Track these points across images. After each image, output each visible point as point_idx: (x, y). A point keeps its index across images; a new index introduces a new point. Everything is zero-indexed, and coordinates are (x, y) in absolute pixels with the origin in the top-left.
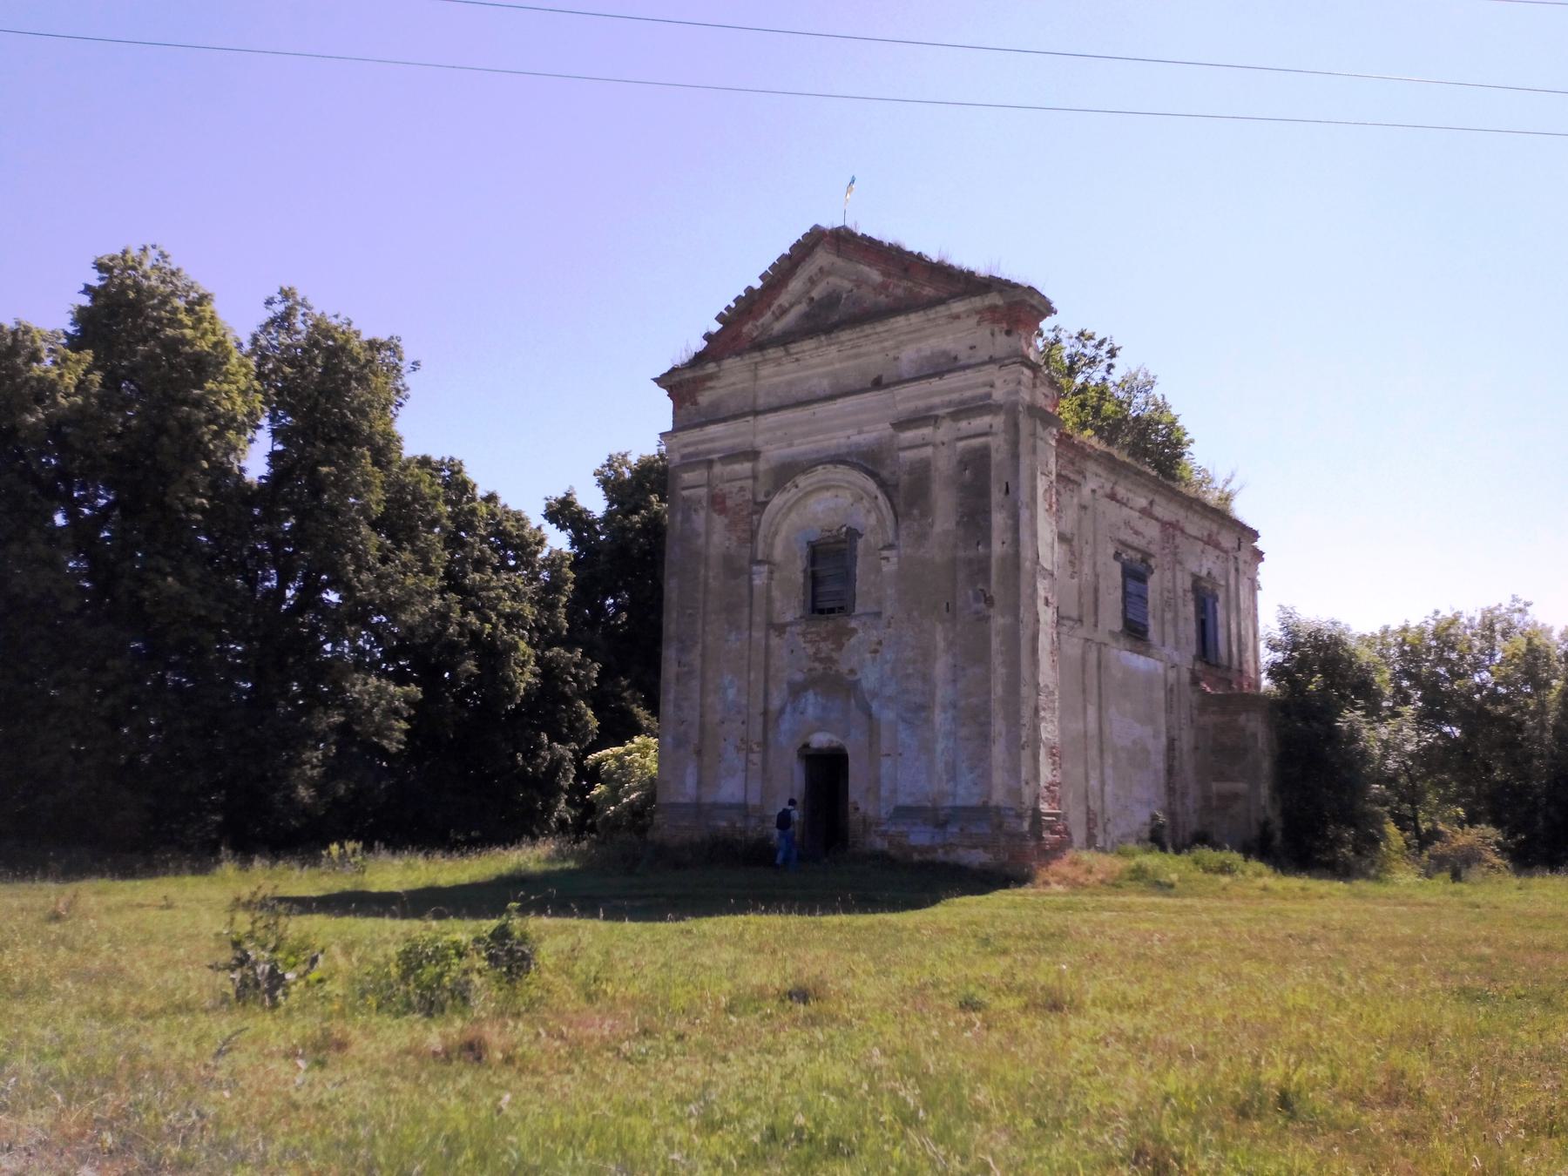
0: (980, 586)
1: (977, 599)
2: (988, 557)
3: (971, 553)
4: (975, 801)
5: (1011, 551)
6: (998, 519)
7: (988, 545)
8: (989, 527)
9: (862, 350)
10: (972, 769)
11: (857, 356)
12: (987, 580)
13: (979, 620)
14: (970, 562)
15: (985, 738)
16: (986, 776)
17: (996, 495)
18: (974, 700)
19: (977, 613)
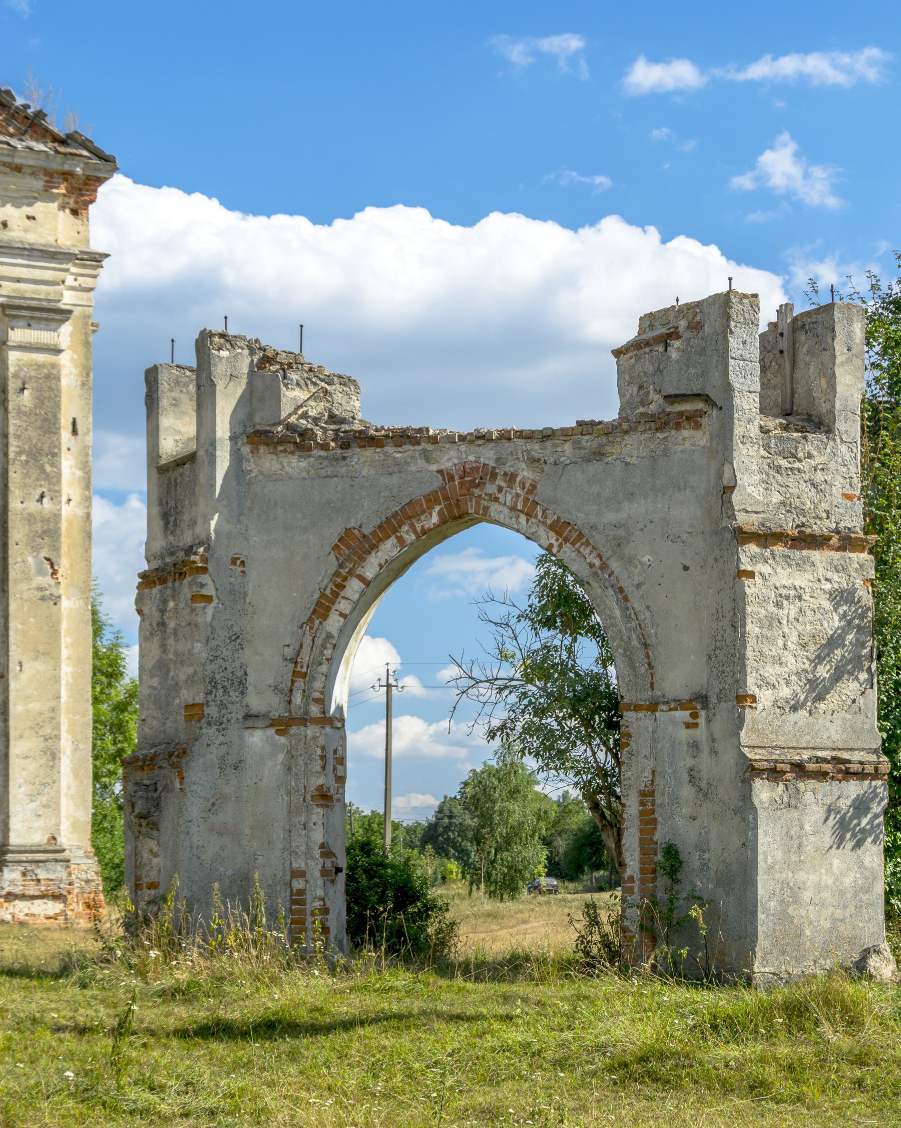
0: (43, 554)
1: (40, 572)
2: (57, 516)
3: (33, 506)
4: (38, 838)
5: (81, 512)
6: (68, 465)
7: (56, 496)
8: (59, 475)
10: (32, 797)
12: (56, 549)
13: (43, 599)
14: (30, 519)
15: (54, 756)
16: (53, 805)
17: (65, 434)
18: (35, 706)
19: (40, 589)
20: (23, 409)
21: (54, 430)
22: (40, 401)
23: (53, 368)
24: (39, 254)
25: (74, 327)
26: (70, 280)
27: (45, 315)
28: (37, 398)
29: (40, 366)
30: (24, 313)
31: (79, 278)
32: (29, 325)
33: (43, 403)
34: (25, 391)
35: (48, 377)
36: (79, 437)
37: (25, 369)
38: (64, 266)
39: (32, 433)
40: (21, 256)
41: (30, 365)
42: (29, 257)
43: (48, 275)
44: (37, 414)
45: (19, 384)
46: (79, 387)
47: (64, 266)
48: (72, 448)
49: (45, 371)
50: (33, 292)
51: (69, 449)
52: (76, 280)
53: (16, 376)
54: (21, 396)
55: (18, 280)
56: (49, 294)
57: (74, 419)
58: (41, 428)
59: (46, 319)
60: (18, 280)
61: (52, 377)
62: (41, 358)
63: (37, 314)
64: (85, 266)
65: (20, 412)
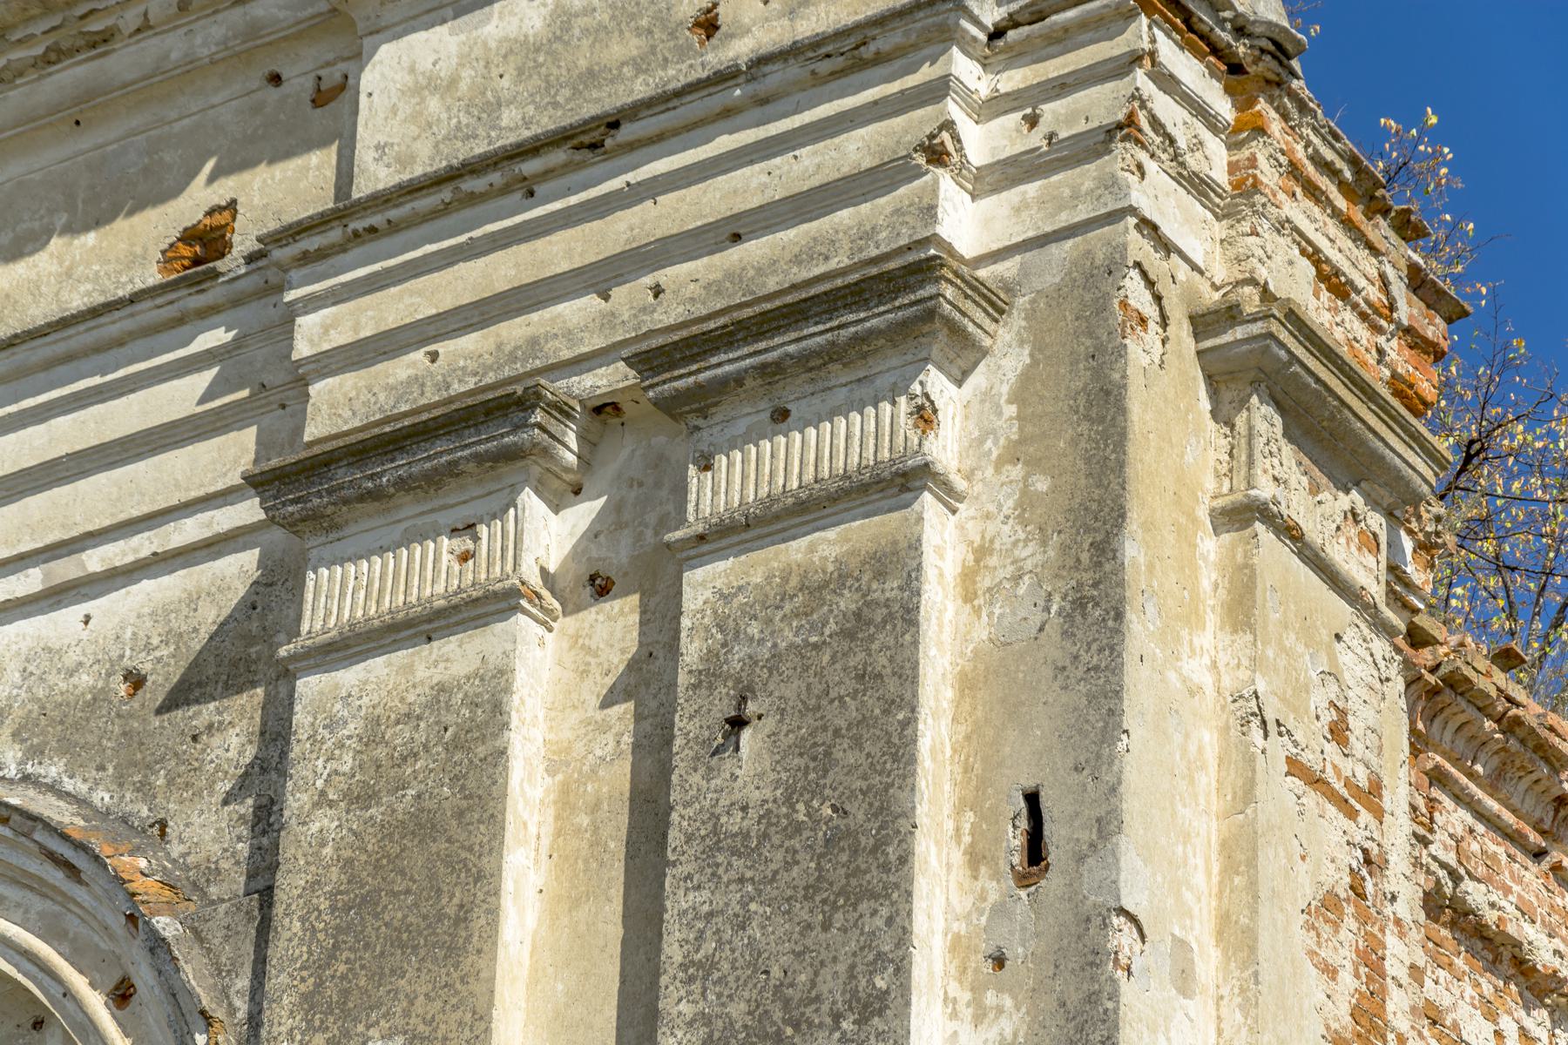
9: (123, 62)
11: (77, 114)
20: (733, 823)
21: (874, 877)
22: (812, 759)
23: (880, 575)
24: (794, 70)
25: (1038, 348)
26: (981, 142)
27: (815, 335)
28: (801, 748)
29: (816, 588)
30: (725, 364)
31: (1049, 110)
32: (781, 415)
33: (825, 762)
34: (746, 735)
35: (856, 627)
36: (1052, 883)
37: (754, 629)
38: (926, 73)
39: (771, 933)
40: (727, 116)
41: (770, 603)
42: (765, 104)
43: (855, 149)
44: (798, 828)
45: (724, 707)
46: (1053, 631)
47: (926, 73)
48: (1016, 952)
49: (847, 602)
50: (797, 260)
51: (999, 961)
52: (1033, 121)
53: (708, 677)
54: (728, 765)
55: (733, 231)
56: (868, 235)
57: (1032, 799)
58: (810, 891)
59: (833, 355)
60: (733, 231)
61: (877, 616)
62: (825, 546)
63: (783, 345)
64: (1063, 41)
65: (716, 842)
